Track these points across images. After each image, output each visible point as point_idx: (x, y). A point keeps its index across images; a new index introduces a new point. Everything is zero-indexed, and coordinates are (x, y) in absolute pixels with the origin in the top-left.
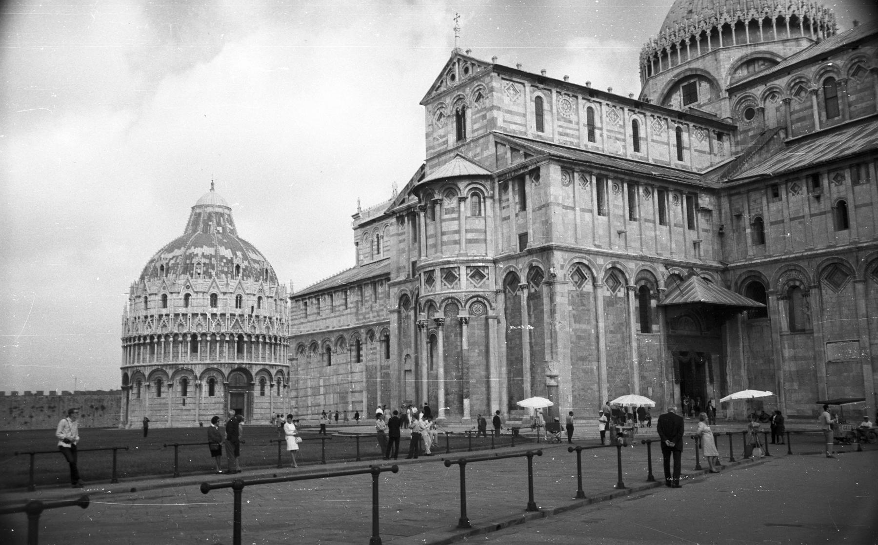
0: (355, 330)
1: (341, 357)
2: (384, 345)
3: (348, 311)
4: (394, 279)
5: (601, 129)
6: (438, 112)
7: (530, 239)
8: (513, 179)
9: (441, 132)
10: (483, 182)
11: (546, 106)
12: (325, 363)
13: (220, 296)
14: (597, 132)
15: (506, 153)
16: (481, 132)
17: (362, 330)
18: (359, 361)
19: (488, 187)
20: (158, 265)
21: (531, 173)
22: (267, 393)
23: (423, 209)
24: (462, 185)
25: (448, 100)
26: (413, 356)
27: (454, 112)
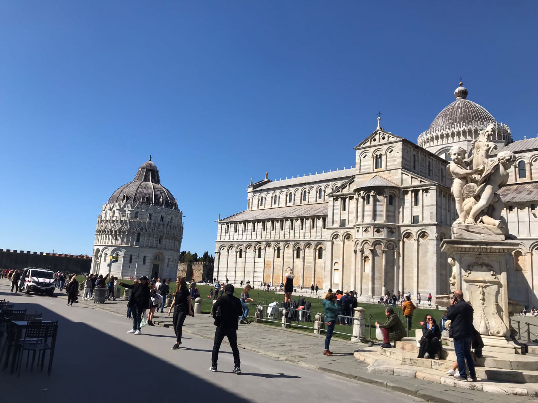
0: (259, 242)
1: (250, 253)
2: (276, 251)
3: (255, 232)
4: (329, 224)
5: (432, 171)
6: (365, 154)
7: (420, 218)
8: (412, 191)
9: (366, 163)
10: (395, 190)
11: (416, 159)
12: (238, 256)
13: (154, 215)
14: (431, 172)
15: (408, 179)
16: (393, 167)
17: (264, 243)
18: (259, 256)
19: (397, 192)
20: (122, 195)
21: (423, 190)
22: (170, 266)
23: (363, 198)
24: (386, 190)
25: (372, 149)
26: (340, 262)
27: (375, 156)
